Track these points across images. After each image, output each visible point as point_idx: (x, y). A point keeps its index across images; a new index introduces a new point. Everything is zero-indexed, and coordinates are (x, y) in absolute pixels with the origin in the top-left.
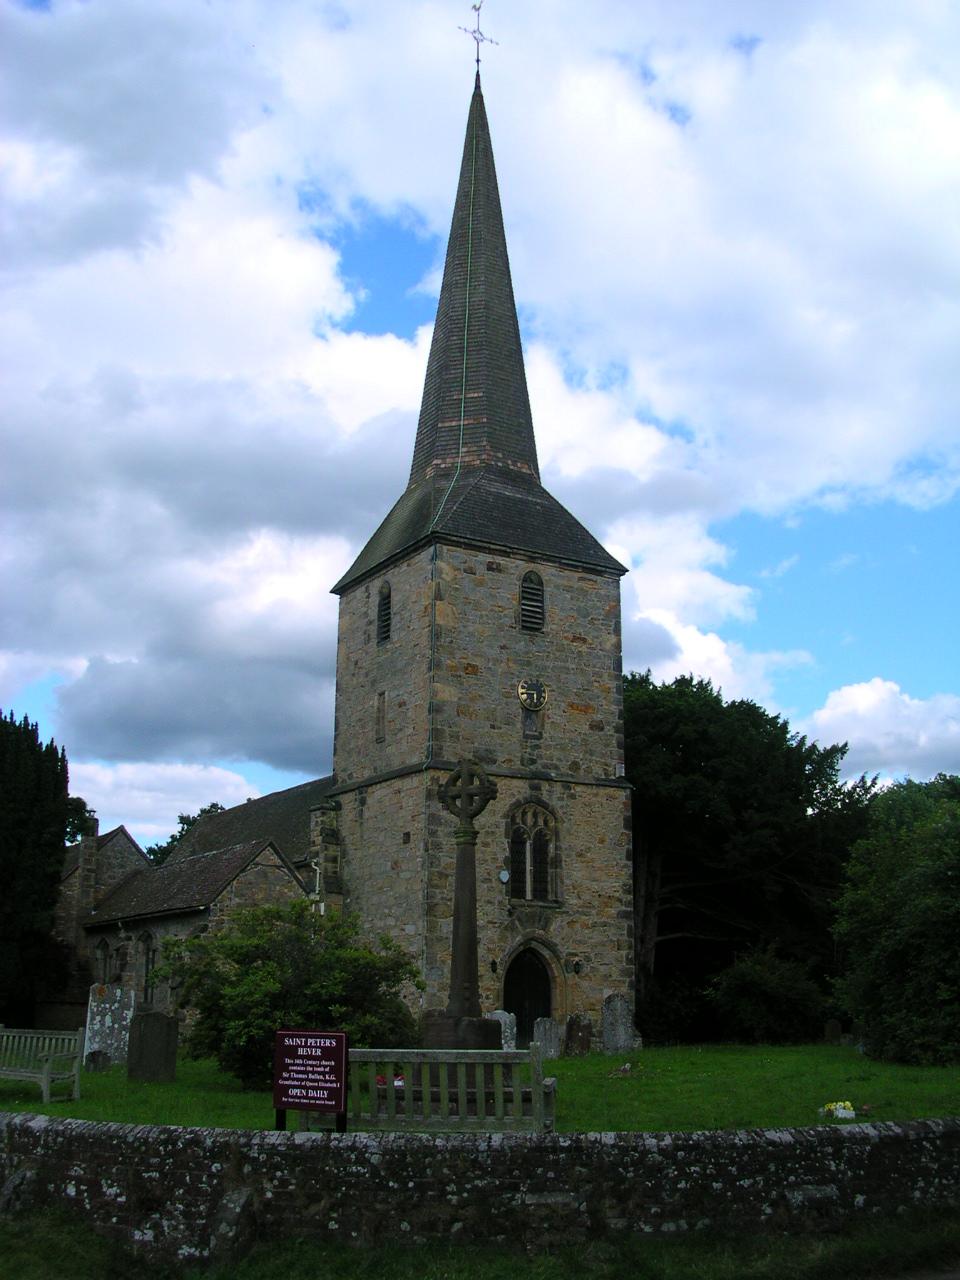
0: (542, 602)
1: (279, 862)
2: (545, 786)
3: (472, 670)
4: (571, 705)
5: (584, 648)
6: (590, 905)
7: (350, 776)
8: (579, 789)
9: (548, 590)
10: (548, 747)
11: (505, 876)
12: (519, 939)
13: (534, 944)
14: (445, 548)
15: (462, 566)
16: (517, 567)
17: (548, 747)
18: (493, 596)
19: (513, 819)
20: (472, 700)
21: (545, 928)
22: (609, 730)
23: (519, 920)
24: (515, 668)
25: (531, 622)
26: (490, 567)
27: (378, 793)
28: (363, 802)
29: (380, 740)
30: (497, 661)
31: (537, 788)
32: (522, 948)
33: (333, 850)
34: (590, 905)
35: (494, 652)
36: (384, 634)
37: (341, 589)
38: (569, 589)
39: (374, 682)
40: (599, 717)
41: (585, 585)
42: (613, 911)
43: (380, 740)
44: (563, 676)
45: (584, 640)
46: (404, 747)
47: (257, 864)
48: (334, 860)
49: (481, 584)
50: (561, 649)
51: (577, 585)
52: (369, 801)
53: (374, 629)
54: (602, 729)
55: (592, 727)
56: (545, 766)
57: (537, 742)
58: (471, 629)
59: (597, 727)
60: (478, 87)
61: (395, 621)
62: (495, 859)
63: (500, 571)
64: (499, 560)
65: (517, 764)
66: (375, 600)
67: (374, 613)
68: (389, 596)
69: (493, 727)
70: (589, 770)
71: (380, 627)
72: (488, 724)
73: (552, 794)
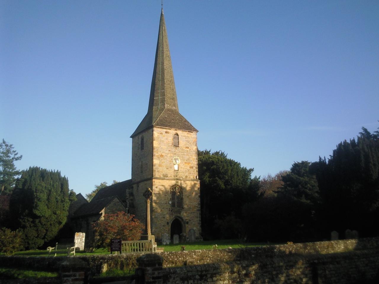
0: (178, 140)
1: (119, 201)
3: (162, 156)
5: (188, 150)
7: (135, 180)
10: (180, 173)
11: (170, 203)
12: (174, 216)
13: (178, 218)
15: (160, 133)
16: (172, 132)
17: (180, 173)
18: (167, 139)
20: (162, 163)
21: (180, 214)
22: (194, 168)
23: (174, 212)
24: (172, 155)
26: (166, 133)
27: (141, 184)
28: (138, 186)
29: (142, 172)
32: (174, 219)
33: (131, 198)
35: (167, 152)
36: (142, 148)
38: (185, 136)
39: (140, 159)
40: (192, 165)
41: (188, 135)
42: (196, 209)
43: (142, 172)
44: (184, 156)
45: (188, 148)
47: (114, 202)
48: (132, 200)
49: (164, 136)
51: (186, 135)
52: (140, 186)
53: (140, 147)
54: (193, 168)
56: (180, 177)
57: (177, 172)
58: (162, 147)
59: (192, 167)
60: (162, 14)
61: (145, 145)
63: (168, 133)
64: (168, 130)
65: (173, 177)
66: (140, 140)
67: (140, 143)
68: (143, 139)
69: (167, 169)
70: (190, 177)
71: (141, 146)
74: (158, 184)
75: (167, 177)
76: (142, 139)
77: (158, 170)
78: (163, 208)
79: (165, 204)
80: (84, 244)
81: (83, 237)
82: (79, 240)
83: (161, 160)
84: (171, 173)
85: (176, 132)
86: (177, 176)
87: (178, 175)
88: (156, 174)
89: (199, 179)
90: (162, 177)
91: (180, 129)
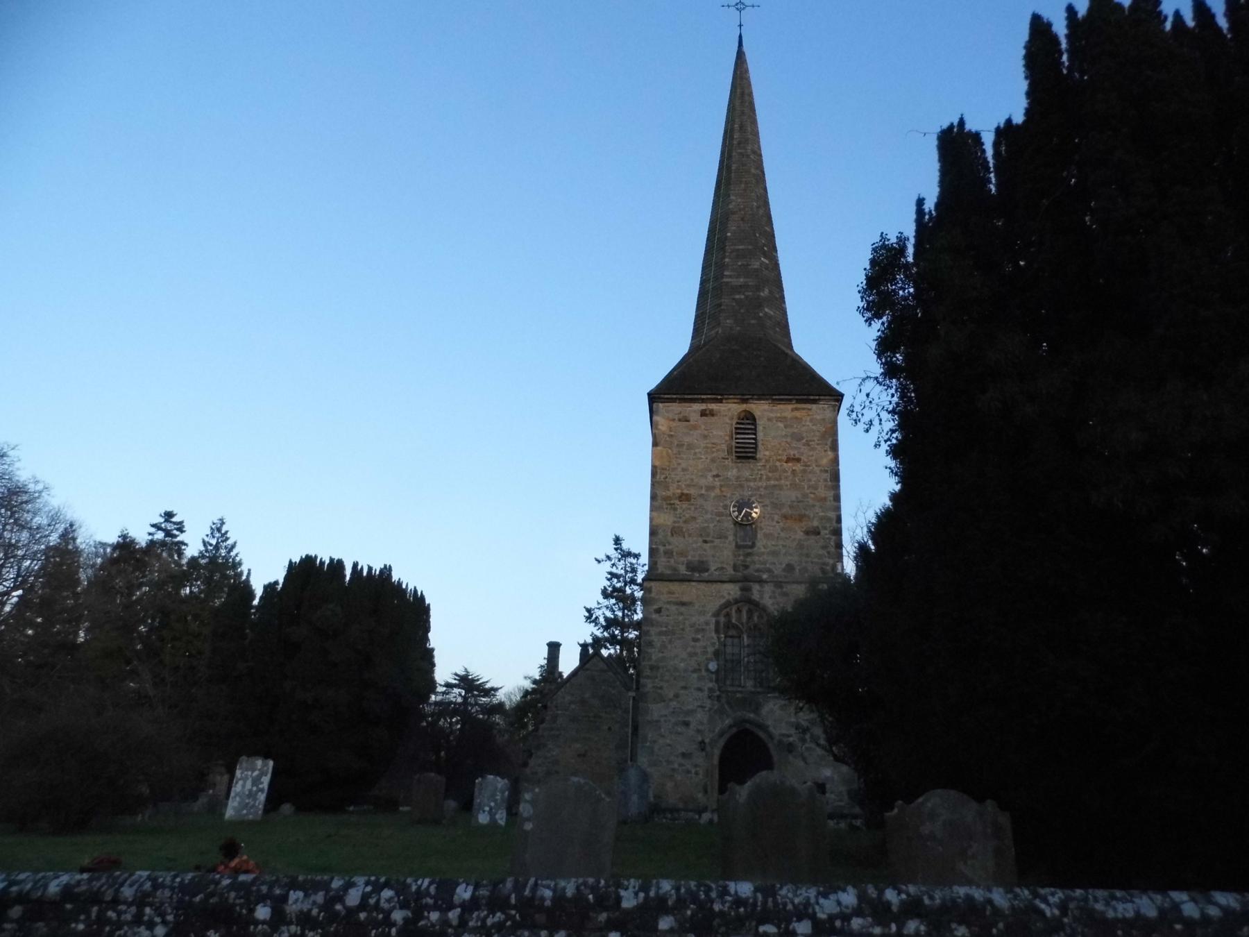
2: (756, 588)
3: (684, 497)
4: (785, 517)
5: (798, 467)
9: (761, 424)
12: (728, 722)
13: (748, 726)
14: (661, 405)
16: (730, 409)
18: (705, 437)
19: (728, 615)
20: (685, 522)
21: (757, 709)
23: (728, 703)
26: (703, 413)
30: (710, 488)
32: (734, 730)
40: (816, 523)
41: (797, 414)
45: (798, 460)
49: (695, 427)
50: (774, 469)
51: (788, 414)
54: (819, 533)
55: (807, 533)
56: (758, 571)
58: (684, 465)
60: (740, 55)
62: (705, 653)
64: (713, 406)
65: (730, 571)
69: (705, 542)
72: (700, 540)
74: (664, 597)
75: (707, 570)
77: (668, 547)
78: (685, 688)
79: (695, 671)
80: (262, 797)
81: (263, 774)
82: (249, 784)
83: (679, 511)
85: (744, 406)
86: (746, 567)
87: (754, 562)
90: (683, 570)
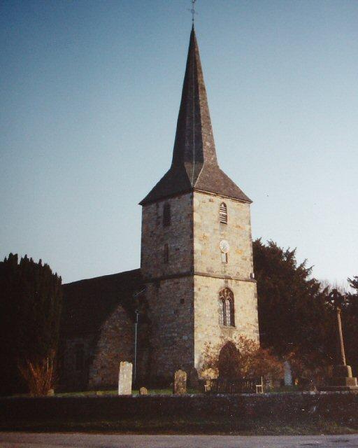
3: (204, 237)
6: (245, 327)
7: (150, 276)
8: (240, 282)
16: (218, 200)
22: (248, 260)
25: (224, 221)
26: (210, 201)
27: (167, 283)
31: (226, 282)
34: (245, 327)
37: (143, 203)
39: (162, 240)
41: (239, 207)
43: (166, 261)
46: (179, 266)
52: (162, 286)
53: (161, 220)
60: (193, 29)
66: (161, 209)
67: (161, 214)
73: (232, 285)
76: (167, 209)
84: (217, 268)
86: (225, 272)
88: (198, 267)
89: (256, 278)
91: (229, 197)
